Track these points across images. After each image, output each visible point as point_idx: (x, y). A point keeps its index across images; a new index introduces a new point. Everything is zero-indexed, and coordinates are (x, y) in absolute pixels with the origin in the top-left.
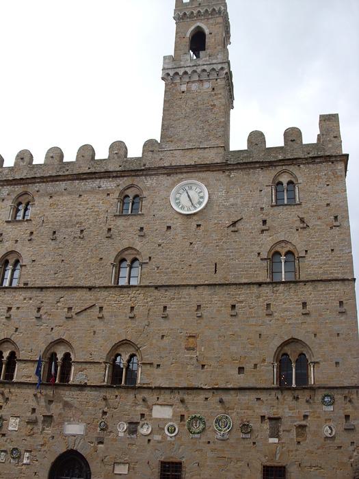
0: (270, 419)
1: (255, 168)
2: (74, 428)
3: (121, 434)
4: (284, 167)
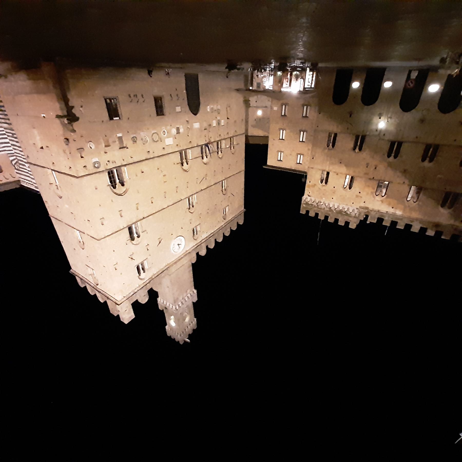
0: (125, 147)
1: (157, 273)
2: (197, 125)
3: (181, 126)
4: (145, 281)
